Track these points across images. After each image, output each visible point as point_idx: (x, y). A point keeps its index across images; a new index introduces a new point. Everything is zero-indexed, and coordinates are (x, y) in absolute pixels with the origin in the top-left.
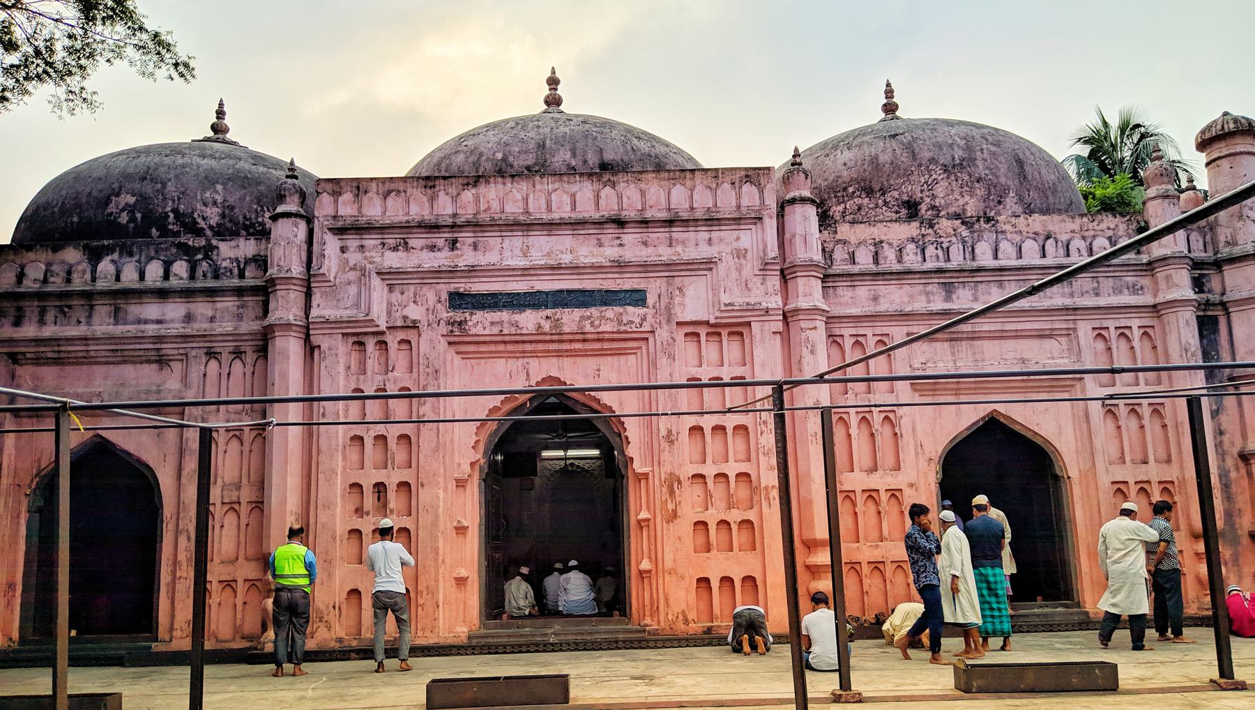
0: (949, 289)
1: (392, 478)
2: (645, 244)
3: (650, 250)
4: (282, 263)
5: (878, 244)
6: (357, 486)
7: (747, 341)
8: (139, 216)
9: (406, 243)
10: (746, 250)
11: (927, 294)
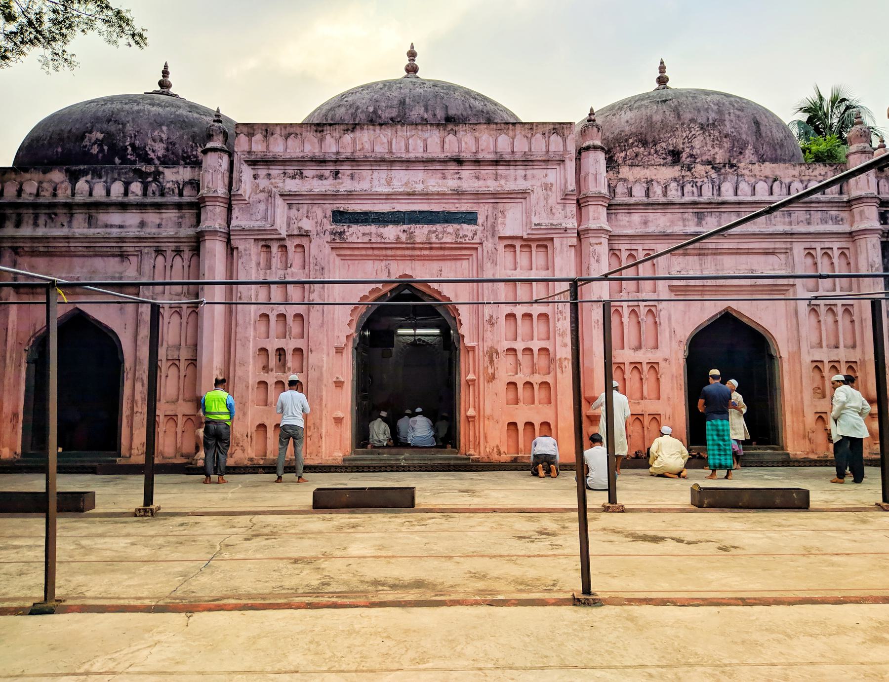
0: (700, 217)
1: (290, 345)
2: (478, 178)
3: (481, 183)
4: (210, 186)
5: (649, 182)
6: (264, 350)
7: (550, 252)
8: (106, 148)
9: (302, 173)
10: (552, 185)
11: (684, 220)
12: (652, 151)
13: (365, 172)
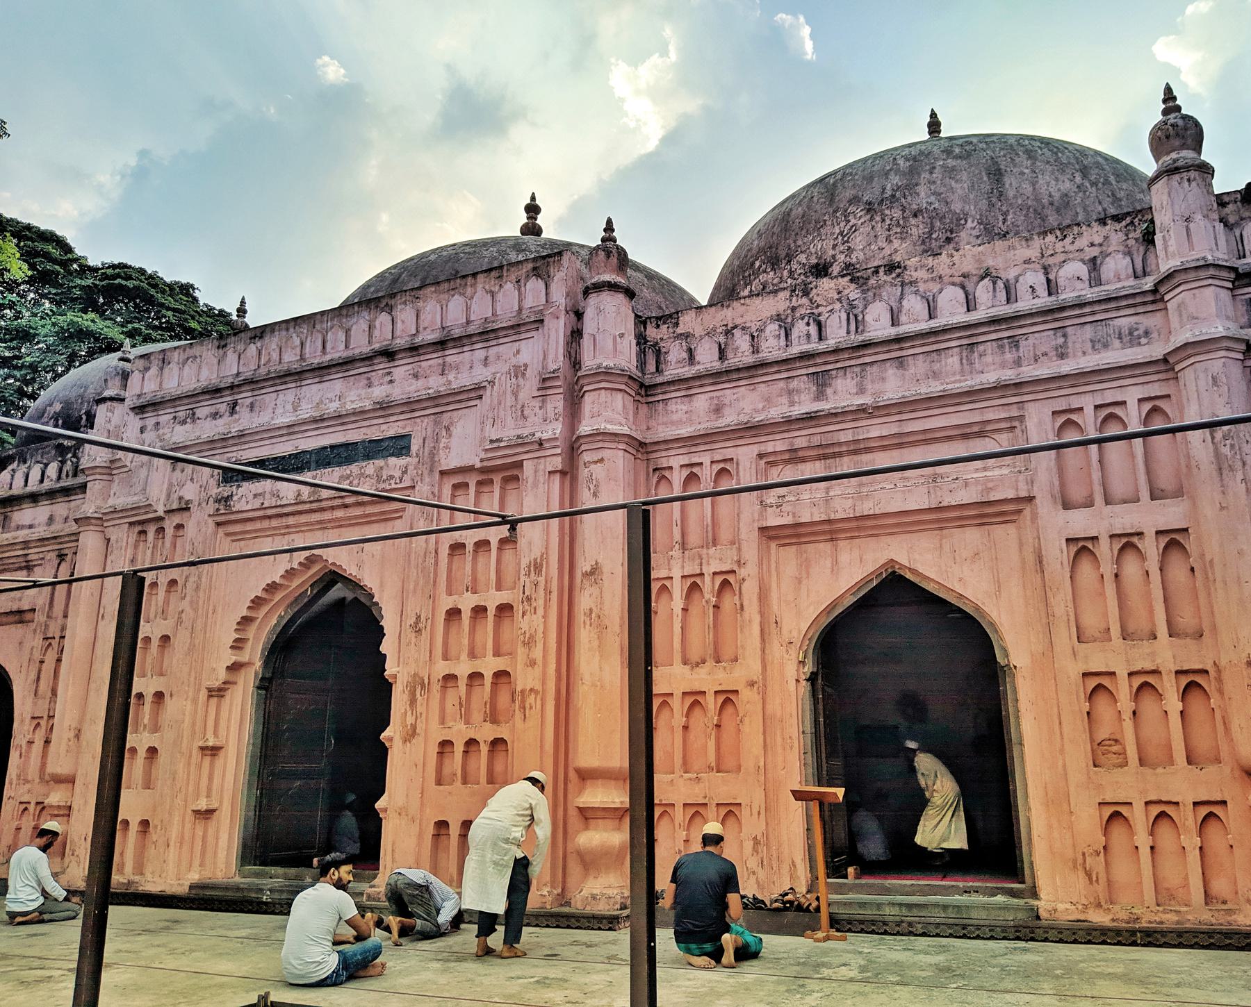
0: (821, 381)
2: (416, 376)
3: (420, 383)
10: (526, 366)
11: (790, 392)
12: (786, 273)
13: (268, 398)
